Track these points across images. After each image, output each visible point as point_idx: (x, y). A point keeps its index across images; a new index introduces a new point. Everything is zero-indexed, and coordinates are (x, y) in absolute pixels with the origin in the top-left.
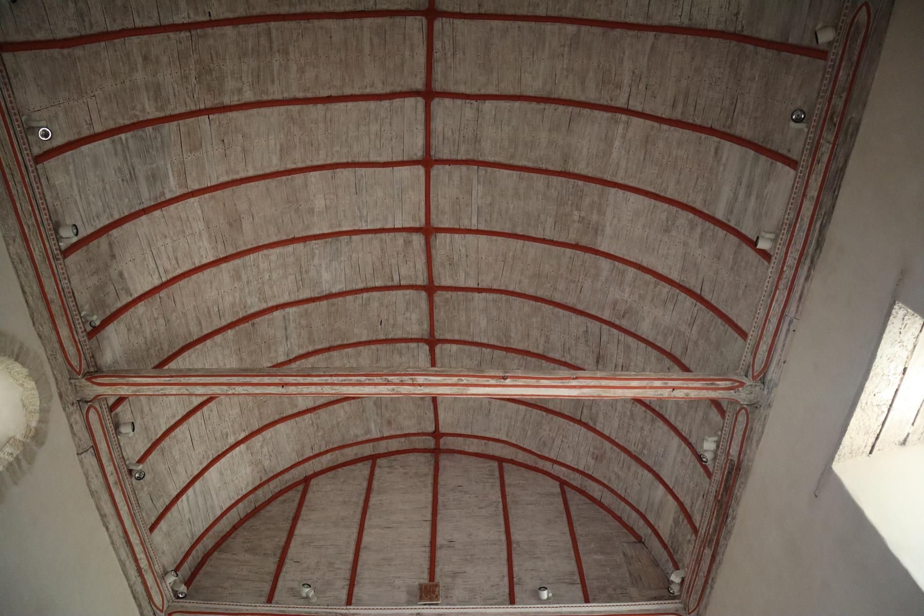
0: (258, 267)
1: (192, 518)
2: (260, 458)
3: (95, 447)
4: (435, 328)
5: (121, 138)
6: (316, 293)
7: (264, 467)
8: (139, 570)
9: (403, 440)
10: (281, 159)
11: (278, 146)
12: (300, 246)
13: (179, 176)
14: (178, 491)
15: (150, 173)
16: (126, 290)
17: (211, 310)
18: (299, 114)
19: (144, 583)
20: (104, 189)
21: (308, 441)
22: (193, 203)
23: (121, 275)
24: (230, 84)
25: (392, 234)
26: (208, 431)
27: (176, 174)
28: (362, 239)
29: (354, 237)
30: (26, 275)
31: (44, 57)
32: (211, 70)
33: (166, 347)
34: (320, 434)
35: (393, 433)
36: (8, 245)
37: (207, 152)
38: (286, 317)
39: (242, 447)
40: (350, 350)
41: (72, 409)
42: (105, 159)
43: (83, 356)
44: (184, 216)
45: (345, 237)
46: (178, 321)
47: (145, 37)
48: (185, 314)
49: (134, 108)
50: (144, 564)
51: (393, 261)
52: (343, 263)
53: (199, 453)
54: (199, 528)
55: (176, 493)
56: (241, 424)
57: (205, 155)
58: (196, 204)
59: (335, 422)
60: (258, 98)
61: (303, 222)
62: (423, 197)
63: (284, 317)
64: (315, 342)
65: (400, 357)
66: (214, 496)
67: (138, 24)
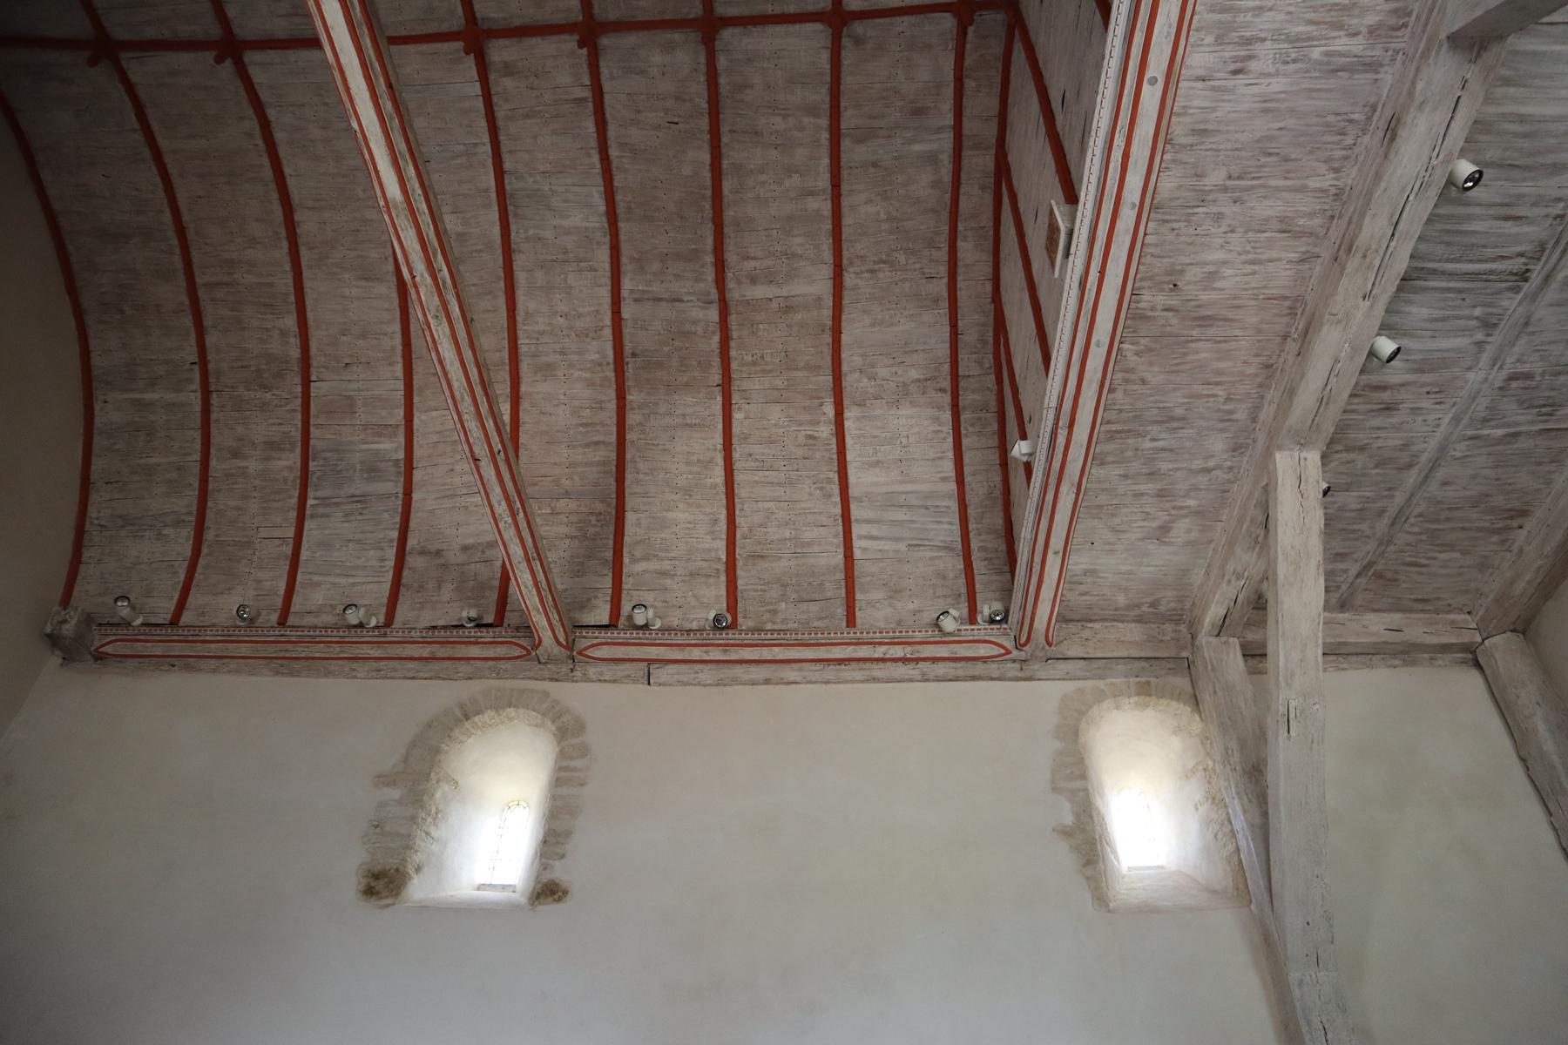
0: (542, 333)
1: (912, 539)
2: (893, 385)
3: (650, 662)
4: (679, 17)
5: (312, 506)
6: (603, 240)
7: (919, 380)
8: (904, 660)
9: (969, 84)
10: (379, 280)
11: (363, 283)
12: (519, 261)
13: (380, 435)
14: (841, 550)
15: (365, 475)
16: (487, 547)
17: (584, 421)
18: (313, 248)
19: (935, 660)
20: (359, 542)
21: (907, 285)
22: (421, 421)
23: (465, 548)
24: (275, 346)
25: (495, 99)
26: (784, 468)
27: (376, 439)
28: (510, 152)
29: (507, 166)
30: (395, 670)
31: (202, 577)
32: (257, 371)
33: (599, 507)
34: (903, 259)
35: (947, 106)
36: (355, 677)
37: (359, 390)
38: (637, 296)
39: (850, 414)
40: (727, 186)
41: (578, 674)
42: (327, 532)
43: (514, 640)
44: (435, 438)
45: (506, 182)
46: (576, 477)
47: (212, 451)
48: (572, 465)
49: (285, 481)
50: (898, 651)
51: (548, 96)
52: (553, 188)
53: (810, 494)
54: (948, 530)
55: (841, 556)
56: (805, 408)
57: (362, 393)
58: (423, 418)
59: (885, 226)
60: (293, 307)
61: (479, 251)
62: (411, 48)
63: (636, 300)
64: (696, 250)
65: (751, 87)
66: (910, 487)
67: (197, 456)
